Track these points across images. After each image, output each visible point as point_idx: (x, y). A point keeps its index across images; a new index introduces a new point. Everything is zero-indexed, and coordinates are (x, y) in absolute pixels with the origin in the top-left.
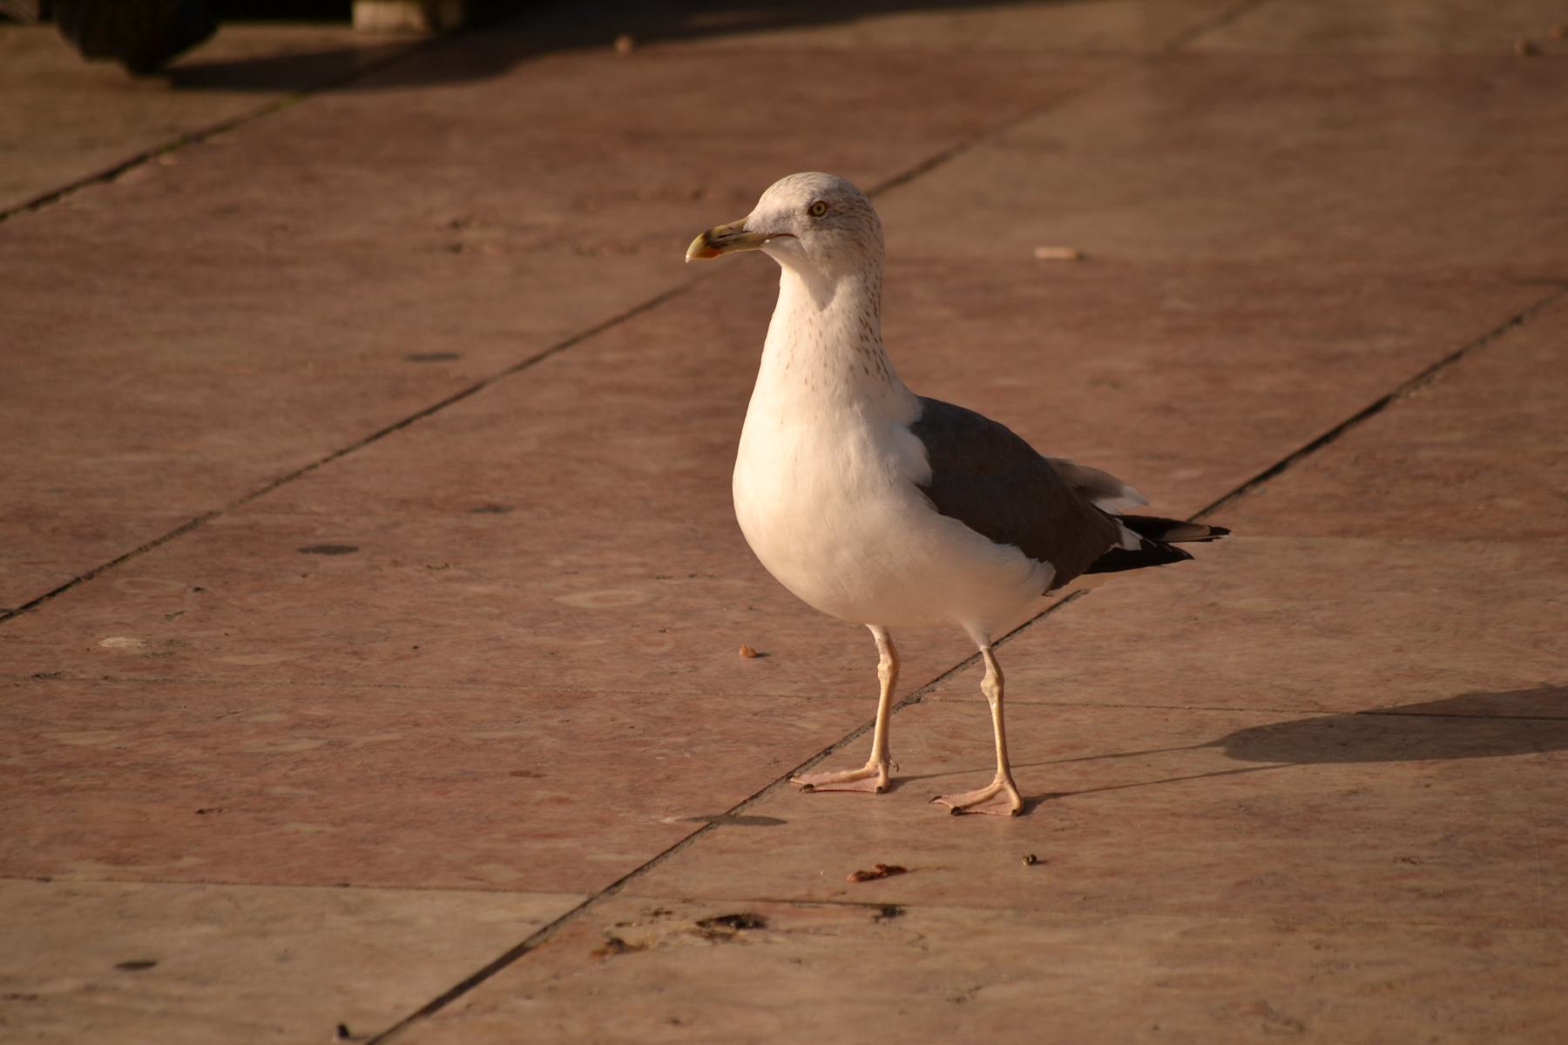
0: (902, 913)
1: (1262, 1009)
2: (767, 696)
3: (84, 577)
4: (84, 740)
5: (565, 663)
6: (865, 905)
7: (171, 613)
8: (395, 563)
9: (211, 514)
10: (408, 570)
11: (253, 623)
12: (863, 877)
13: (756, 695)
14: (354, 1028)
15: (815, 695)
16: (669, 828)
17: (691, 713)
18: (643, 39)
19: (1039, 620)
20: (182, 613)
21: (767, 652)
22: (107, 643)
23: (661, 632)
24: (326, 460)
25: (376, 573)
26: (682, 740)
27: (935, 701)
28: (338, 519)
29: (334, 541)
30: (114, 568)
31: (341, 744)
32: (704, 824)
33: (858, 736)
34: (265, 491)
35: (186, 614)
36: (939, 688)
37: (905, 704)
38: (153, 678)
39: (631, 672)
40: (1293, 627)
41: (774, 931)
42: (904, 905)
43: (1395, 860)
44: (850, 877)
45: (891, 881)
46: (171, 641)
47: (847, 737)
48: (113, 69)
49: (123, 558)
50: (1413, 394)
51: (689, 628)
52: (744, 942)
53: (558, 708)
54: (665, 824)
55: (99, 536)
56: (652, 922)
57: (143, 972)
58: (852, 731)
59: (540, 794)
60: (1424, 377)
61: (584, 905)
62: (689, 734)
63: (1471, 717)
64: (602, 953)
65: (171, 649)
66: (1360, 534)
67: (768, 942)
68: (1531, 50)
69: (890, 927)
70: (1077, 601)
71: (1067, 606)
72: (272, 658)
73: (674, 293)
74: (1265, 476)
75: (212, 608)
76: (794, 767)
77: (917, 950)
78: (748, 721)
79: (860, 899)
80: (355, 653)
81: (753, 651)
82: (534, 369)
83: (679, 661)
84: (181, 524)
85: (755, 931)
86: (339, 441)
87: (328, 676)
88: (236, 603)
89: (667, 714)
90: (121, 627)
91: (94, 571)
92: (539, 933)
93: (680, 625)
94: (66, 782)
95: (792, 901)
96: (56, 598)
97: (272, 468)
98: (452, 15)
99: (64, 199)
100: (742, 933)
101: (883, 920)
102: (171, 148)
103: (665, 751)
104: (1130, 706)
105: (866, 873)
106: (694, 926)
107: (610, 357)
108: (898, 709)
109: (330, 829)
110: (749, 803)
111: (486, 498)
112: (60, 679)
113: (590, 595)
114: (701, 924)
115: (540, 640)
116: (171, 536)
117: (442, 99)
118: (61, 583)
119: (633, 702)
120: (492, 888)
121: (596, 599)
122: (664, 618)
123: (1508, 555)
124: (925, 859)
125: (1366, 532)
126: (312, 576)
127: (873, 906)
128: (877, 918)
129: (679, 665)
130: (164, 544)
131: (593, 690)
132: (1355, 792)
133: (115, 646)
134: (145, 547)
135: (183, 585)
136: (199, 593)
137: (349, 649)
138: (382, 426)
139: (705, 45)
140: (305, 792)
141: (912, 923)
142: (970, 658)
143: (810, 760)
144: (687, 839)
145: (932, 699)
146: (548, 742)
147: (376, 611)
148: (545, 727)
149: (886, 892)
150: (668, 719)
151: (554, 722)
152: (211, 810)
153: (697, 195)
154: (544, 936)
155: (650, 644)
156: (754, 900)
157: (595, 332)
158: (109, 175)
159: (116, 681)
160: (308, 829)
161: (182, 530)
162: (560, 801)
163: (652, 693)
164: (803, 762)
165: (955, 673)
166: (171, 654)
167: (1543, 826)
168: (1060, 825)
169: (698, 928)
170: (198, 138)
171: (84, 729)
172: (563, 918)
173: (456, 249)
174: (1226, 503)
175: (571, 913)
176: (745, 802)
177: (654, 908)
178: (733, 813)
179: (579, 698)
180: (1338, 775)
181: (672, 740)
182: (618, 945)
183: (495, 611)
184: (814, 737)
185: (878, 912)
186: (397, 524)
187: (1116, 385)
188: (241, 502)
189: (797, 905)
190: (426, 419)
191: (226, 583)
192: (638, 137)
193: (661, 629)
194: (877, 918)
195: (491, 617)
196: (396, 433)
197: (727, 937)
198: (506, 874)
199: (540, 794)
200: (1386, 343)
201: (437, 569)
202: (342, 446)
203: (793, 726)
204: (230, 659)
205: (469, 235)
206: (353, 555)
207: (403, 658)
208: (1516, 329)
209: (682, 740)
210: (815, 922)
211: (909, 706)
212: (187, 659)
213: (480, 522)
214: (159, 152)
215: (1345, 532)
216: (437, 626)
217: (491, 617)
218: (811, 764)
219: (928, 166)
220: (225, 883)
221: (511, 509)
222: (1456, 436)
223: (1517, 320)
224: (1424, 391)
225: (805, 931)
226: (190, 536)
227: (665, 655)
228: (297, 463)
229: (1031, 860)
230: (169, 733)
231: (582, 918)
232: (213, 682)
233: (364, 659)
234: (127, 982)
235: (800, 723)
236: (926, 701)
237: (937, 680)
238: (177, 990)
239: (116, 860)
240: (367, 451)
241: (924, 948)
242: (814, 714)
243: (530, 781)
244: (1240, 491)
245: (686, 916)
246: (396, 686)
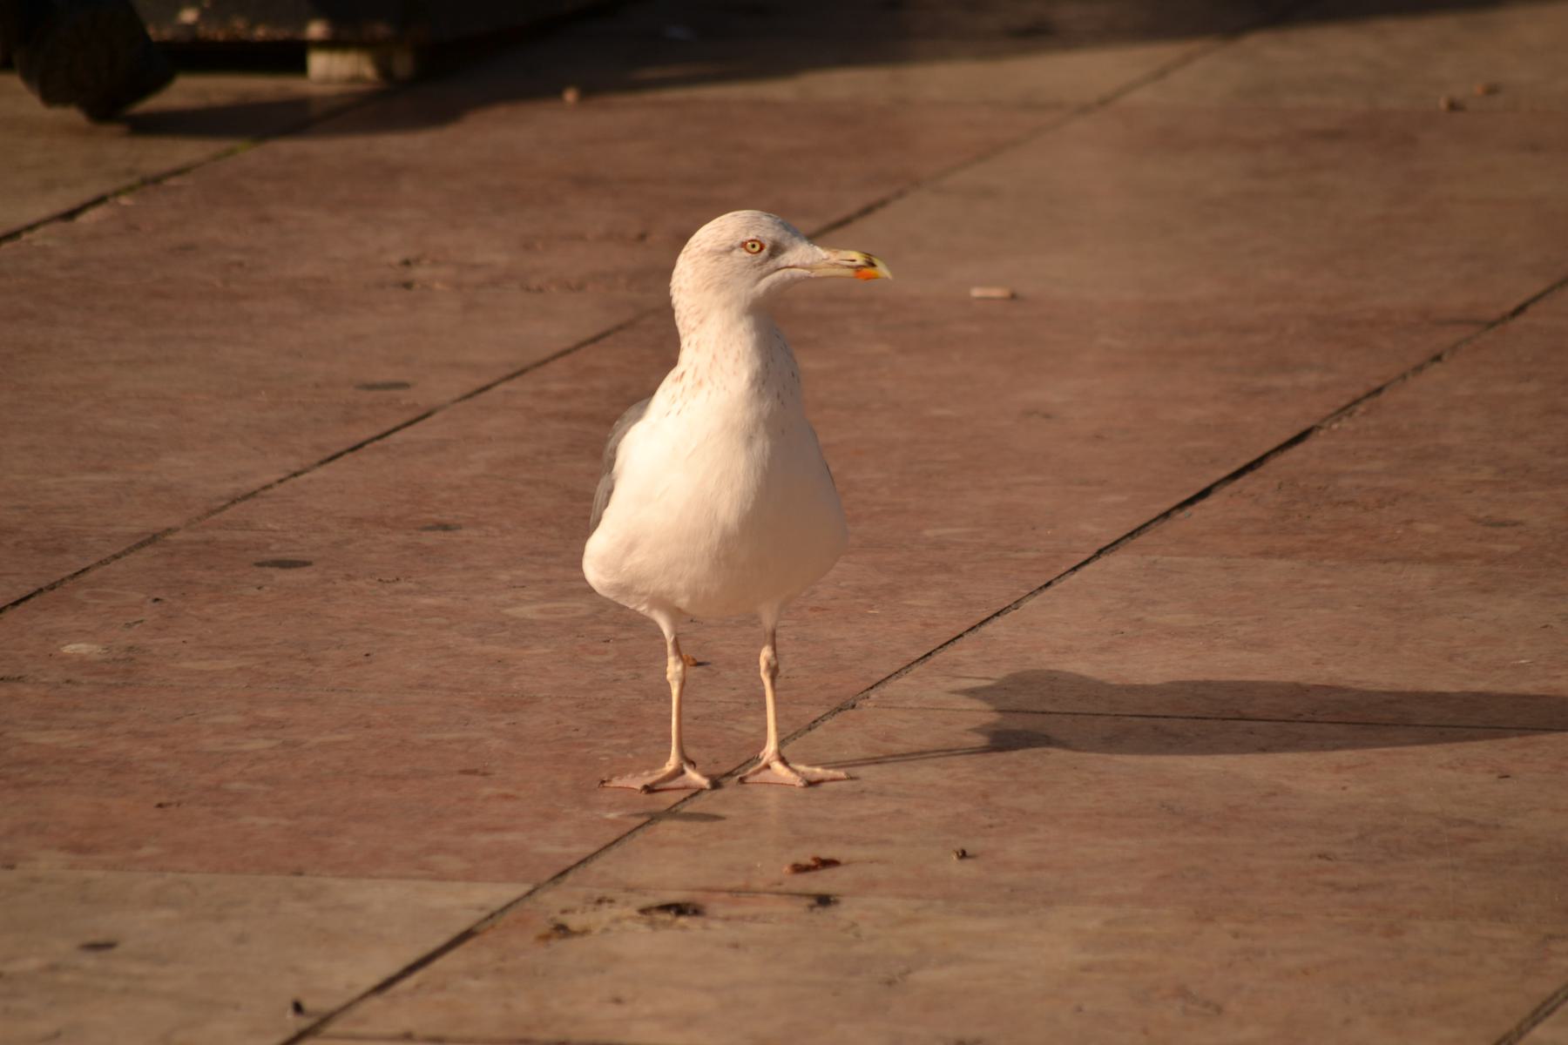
0: (836, 902)
1: (1182, 992)
2: (707, 701)
3: (47, 588)
4: (46, 739)
5: (512, 670)
6: (800, 895)
7: (130, 622)
8: (349, 577)
9: (169, 531)
10: (360, 584)
11: (210, 631)
12: (799, 869)
13: (697, 701)
14: (308, 1004)
15: (753, 700)
16: (613, 823)
17: (633, 716)
18: (589, 91)
19: (970, 633)
20: (141, 621)
21: (708, 660)
22: (69, 649)
23: (605, 642)
24: (281, 481)
25: (329, 585)
26: (625, 742)
27: (869, 707)
28: (292, 536)
29: (289, 556)
30: (76, 580)
31: (295, 744)
32: (645, 819)
33: (795, 739)
34: (224, 508)
35: (144, 623)
36: (873, 695)
37: (840, 710)
38: (113, 682)
39: (575, 679)
40: (1216, 641)
41: (714, 918)
42: (837, 895)
43: (1311, 857)
44: (786, 869)
45: (826, 873)
46: (131, 647)
47: (783, 740)
48: (72, 115)
49: (84, 571)
50: (1335, 426)
51: (632, 638)
52: (684, 928)
53: (504, 711)
54: (607, 820)
55: (62, 550)
56: (595, 910)
57: (103, 953)
58: (789, 734)
59: (488, 791)
60: (1346, 410)
61: (529, 894)
62: (631, 736)
63: (1387, 725)
64: (545, 938)
65: (131, 654)
66: (1281, 556)
67: (706, 928)
68: (1453, 106)
69: (823, 915)
70: (1008, 615)
71: (998, 620)
72: (229, 664)
73: (620, 328)
74: (1190, 502)
75: (171, 617)
76: (735, 766)
77: (850, 936)
78: (690, 724)
79: (797, 889)
80: (309, 660)
81: (694, 659)
82: (483, 399)
83: (620, 669)
84: (140, 540)
85: (694, 918)
86: (293, 463)
87: (283, 681)
88: (193, 613)
89: (610, 717)
90: (82, 634)
91: (56, 582)
92: (486, 919)
93: (624, 635)
94: (30, 777)
95: (730, 891)
96: (19, 608)
97: (229, 488)
98: (403, 65)
99: (25, 236)
100: (683, 920)
101: (818, 909)
102: (130, 189)
103: (606, 752)
104: (1058, 713)
105: (800, 865)
106: (635, 913)
107: (556, 387)
108: (833, 715)
109: (285, 822)
110: (689, 801)
111: (435, 516)
112: (23, 682)
113: (535, 607)
114: (644, 911)
115: (488, 648)
116: (130, 550)
117: (394, 146)
118: (25, 594)
119: (577, 706)
120: (442, 877)
121: (542, 611)
122: (608, 629)
123: (1424, 576)
124: (858, 852)
125: (1284, 555)
126: (267, 588)
127: (808, 896)
128: (811, 907)
129: (622, 672)
130: (124, 558)
131: (541, 695)
132: (1274, 794)
133: (77, 652)
134: (106, 560)
135: (142, 596)
136: (157, 604)
137: (303, 656)
138: (336, 450)
139: (650, 96)
140: (261, 787)
141: (846, 912)
142: (904, 668)
143: (748, 762)
144: (629, 833)
145: (867, 706)
146: (495, 743)
147: (330, 621)
148: (492, 729)
149: (820, 882)
150: (611, 722)
151: (501, 725)
152: (170, 804)
153: (642, 237)
154: (491, 921)
155: (595, 653)
156: (694, 890)
157: (545, 362)
158: (70, 215)
159: (78, 684)
160: (263, 822)
161: (141, 545)
162: (506, 797)
163: (596, 699)
164: (742, 762)
165: (888, 681)
166: (132, 659)
167: (1454, 826)
168: (987, 821)
169: (639, 915)
170: (157, 180)
171: (47, 728)
172: (509, 906)
173: (408, 285)
174: (1153, 525)
175: (517, 901)
176: (685, 799)
177: (596, 897)
178: (674, 809)
179: (525, 703)
180: (1257, 768)
181: (615, 742)
182: (562, 930)
183: (444, 621)
184: (752, 739)
185: (813, 902)
186: (349, 541)
187: (1047, 416)
188: (199, 519)
189: (734, 895)
190: (378, 443)
191: (184, 594)
192: (584, 182)
193: (605, 639)
194: (811, 907)
195: (440, 627)
196: (348, 456)
197: (667, 925)
198: (453, 864)
199: (488, 791)
200: (1310, 378)
201: (388, 582)
202: (298, 469)
203: (733, 729)
204: (187, 665)
205: (419, 273)
206: (307, 569)
207: (355, 664)
208: (1437, 365)
209: (625, 742)
210: (750, 910)
211: (844, 712)
212: (147, 664)
213: (430, 539)
214: (117, 194)
215: (1266, 554)
216: (388, 635)
217: (440, 627)
218: (748, 765)
219: (867, 211)
220: (183, 871)
221: (460, 527)
222: (1377, 465)
223: (1438, 358)
224: (1346, 423)
225: (742, 918)
226: (149, 550)
227: (608, 663)
228: (252, 484)
229: (960, 854)
230: (129, 732)
231: (528, 904)
232: (172, 686)
233: (317, 666)
234: (90, 961)
235: (738, 727)
236: (861, 707)
237: (872, 688)
238: (137, 969)
239: (78, 849)
240: (321, 472)
241: (858, 935)
242: (751, 718)
243: (477, 778)
244: (1166, 515)
245: (627, 904)
246: (348, 690)
